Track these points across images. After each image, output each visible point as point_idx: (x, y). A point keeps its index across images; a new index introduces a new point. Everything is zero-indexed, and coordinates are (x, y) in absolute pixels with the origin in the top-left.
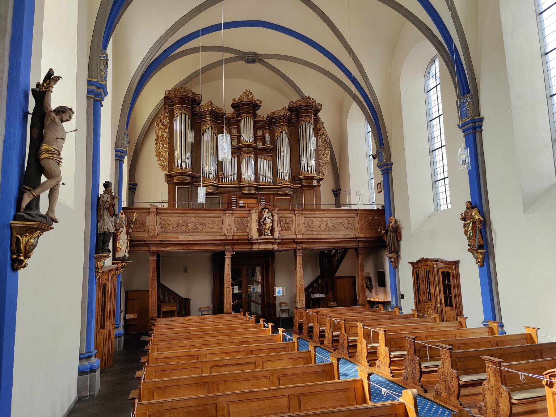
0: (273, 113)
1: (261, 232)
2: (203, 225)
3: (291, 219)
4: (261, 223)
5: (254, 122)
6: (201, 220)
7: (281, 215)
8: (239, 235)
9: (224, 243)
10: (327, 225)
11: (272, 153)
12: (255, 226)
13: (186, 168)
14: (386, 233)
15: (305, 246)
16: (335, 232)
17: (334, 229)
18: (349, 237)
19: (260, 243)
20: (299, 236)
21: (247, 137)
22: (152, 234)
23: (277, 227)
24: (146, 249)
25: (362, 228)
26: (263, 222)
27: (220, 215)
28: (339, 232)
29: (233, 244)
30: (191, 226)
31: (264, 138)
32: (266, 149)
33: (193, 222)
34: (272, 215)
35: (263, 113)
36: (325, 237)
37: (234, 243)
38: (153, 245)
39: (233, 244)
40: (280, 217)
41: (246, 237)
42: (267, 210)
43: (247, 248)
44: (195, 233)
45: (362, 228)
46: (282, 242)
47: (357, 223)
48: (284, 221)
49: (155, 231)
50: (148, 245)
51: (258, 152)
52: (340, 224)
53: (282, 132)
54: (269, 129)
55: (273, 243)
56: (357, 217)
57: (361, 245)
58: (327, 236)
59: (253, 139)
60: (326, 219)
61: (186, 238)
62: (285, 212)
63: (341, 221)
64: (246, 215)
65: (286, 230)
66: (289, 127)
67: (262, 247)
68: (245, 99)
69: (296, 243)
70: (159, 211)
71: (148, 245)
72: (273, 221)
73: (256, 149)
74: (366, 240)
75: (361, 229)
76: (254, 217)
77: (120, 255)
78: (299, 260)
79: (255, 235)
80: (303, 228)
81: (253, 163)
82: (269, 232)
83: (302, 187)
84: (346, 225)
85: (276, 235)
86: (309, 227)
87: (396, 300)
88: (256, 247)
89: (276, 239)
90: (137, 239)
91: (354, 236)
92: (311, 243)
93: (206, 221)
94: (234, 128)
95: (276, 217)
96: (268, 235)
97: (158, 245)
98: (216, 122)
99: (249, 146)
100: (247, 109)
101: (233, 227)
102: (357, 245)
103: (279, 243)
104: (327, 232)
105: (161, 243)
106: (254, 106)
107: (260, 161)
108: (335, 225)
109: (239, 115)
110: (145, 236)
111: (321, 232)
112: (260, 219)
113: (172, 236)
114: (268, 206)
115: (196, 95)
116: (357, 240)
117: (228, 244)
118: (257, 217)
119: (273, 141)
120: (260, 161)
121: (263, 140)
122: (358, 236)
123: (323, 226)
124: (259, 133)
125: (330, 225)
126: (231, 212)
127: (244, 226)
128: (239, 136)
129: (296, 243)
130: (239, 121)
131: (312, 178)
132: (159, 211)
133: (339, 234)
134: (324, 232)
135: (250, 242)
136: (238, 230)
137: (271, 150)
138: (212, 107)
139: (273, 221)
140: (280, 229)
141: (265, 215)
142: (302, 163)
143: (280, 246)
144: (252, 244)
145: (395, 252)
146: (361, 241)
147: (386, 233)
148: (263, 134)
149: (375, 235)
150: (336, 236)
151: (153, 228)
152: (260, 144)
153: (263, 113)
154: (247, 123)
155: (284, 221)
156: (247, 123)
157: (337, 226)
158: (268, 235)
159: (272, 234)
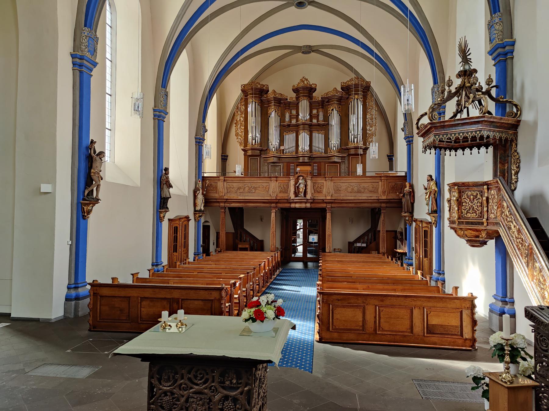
0: (327, 94)
1: (296, 194)
2: (255, 188)
3: (322, 184)
4: (297, 188)
5: (310, 102)
6: (254, 185)
7: (314, 181)
8: (281, 196)
9: (270, 202)
10: (353, 189)
11: (325, 127)
12: (292, 189)
13: (255, 144)
14: (404, 196)
15: (333, 205)
16: (360, 194)
17: (359, 192)
18: (372, 198)
19: (296, 203)
20: (329, 198)
21: (304, 115)
22: (221, 194)
23: (309, 190)
24: (218, 204)
25: (385, 192)
26: (298, 187)
27: (267, 181)
28: (364, 195)
29: (277, 203)
30: (247, 189)
31: (318, 115)
32: (319, 125)
33: (248, 186)
34: (306, 181)
35: (318, 95)
36: (350, 198)
37: (277, 202)
38: (222, 202)
39: (277, 203)
40: (314, 183)
41: (286, 198)
42: (301, 178)
43: (287, 205)
44: (250, 194)
45: (385, 192)
46: (313, 201)
47: (381, 186)
48: (317, 186)
49: (222, 192)
50: (218, 202)
51: (311, 128)
52: (364, 188)
53: (333, 110)
54: (322, 108)
55: (306, 203)
56: (380, 183)
57: (383, 205)
58: (353, 198)
59: (308, 117)
60: (352, 184)
61: (243, 198)
62: (318, 179)
63: (365, 186)
64: (287, 181)
65: (318, 192)
66: (340, 104)
67: (297, 206)
68: (302, 84)
69: (326, 203)
70: (226, 179)
71: (218, 202)
72: (306, 186)
73: (311, 126)
74: (388, 202)
75: (384, 192)
76: (292, 182)
77: (198, 208)
78: (328, 216)
79: (292, 196)
80: (332, 191)
81: (308, 137)
82: (302, 194)
83: (349, 155)
84: (371, 189)
85: (309, 196)
86: (337, 190)
87: (409, 252)
88: (293, 205)
89: (307, 200)
90: (212, 198)
91: (377, 198)
92: (342, 203)
93: (258, 186)
94: (294, 109)
95: (309, 183)
96: (301, 197)
97: (225, 202)
98: (280, 106)
99: (304, 124)
100: (304, 93)
101: (278, 190)
102: (379, 205)
103: (311, 203)
104: (353, 195)
105: (227, 201)
106: (309, 91)
107: (315, 135)
108: (360, 189)
109: (297, 98)
110: (216, 196)
111: (348, 194)
112: (296, 183)
113: (233, 196)
114: (303, 175)
115: (264, 86)
116: (379, 201)
117: (273, 203)
118: (294, 183)
119: (327, 118)
120: (315, 135)
121: (317, 117)
122: (380, 198)
123: (350, 190)
124: (315, 112)
125: (356, 189)
126: (275, 179)
127: (286, 190)
128: (298, 115)
129: (326, 203)
130: (298, 103)
131: (357, 148)
132: (226, 179)
133: (364, 196)
134: (350, 194)
135: (289, 201)
136: (280, 192)
137: (323, 125)
138: (275, 95)
139: (306, 186)
140: (313, 192)
141: (300, 181)
142: (350, 134)
143: (313, 205)
144: (290, 203)
145: (410, 213)
146: (384, 202)
147: (404, 196)
148: (318, 112)
149: (397, 198)
150: (360, 198)
151: (221, 190)
152: (315, 121)
153: (318, 95)
154: (304, 104)
155: (317, 186)
156: (304, 104)
157: (362, 190)
158: (301, 197)
159: (305, 196)
